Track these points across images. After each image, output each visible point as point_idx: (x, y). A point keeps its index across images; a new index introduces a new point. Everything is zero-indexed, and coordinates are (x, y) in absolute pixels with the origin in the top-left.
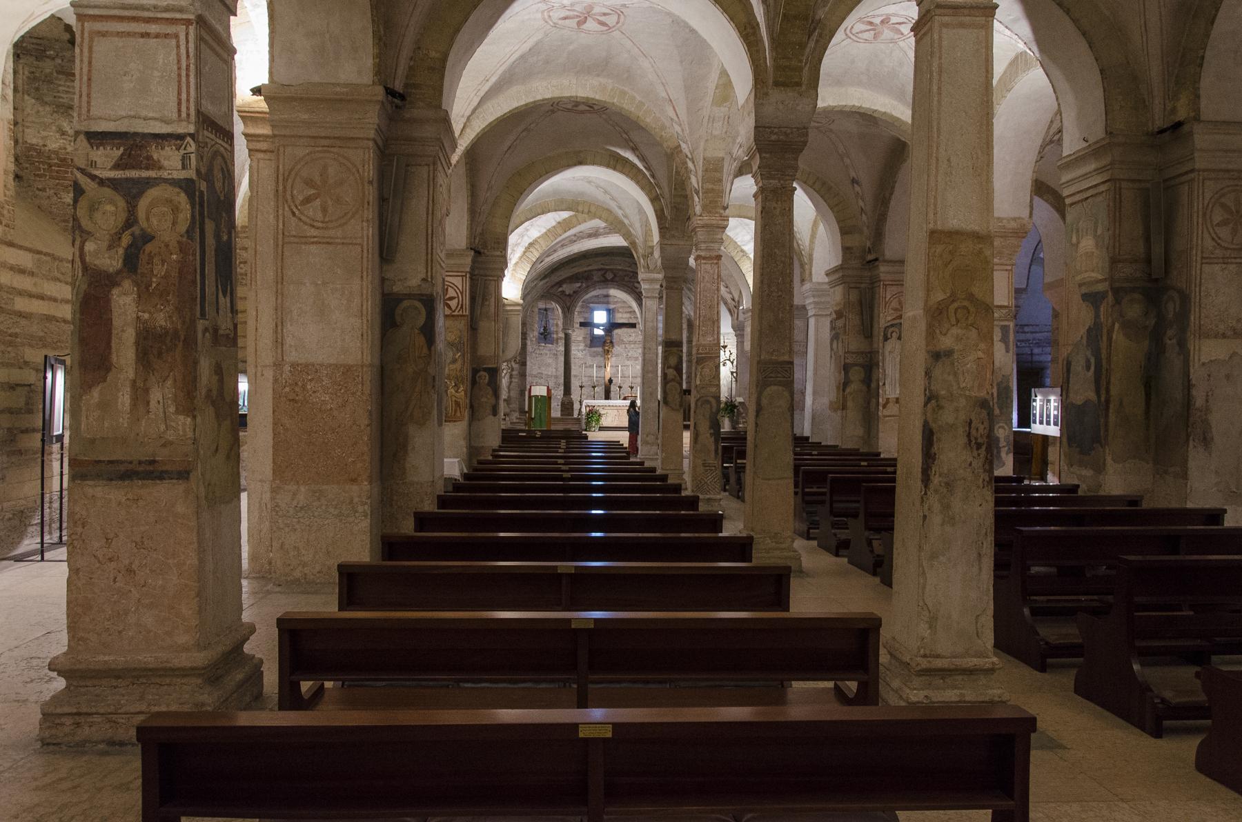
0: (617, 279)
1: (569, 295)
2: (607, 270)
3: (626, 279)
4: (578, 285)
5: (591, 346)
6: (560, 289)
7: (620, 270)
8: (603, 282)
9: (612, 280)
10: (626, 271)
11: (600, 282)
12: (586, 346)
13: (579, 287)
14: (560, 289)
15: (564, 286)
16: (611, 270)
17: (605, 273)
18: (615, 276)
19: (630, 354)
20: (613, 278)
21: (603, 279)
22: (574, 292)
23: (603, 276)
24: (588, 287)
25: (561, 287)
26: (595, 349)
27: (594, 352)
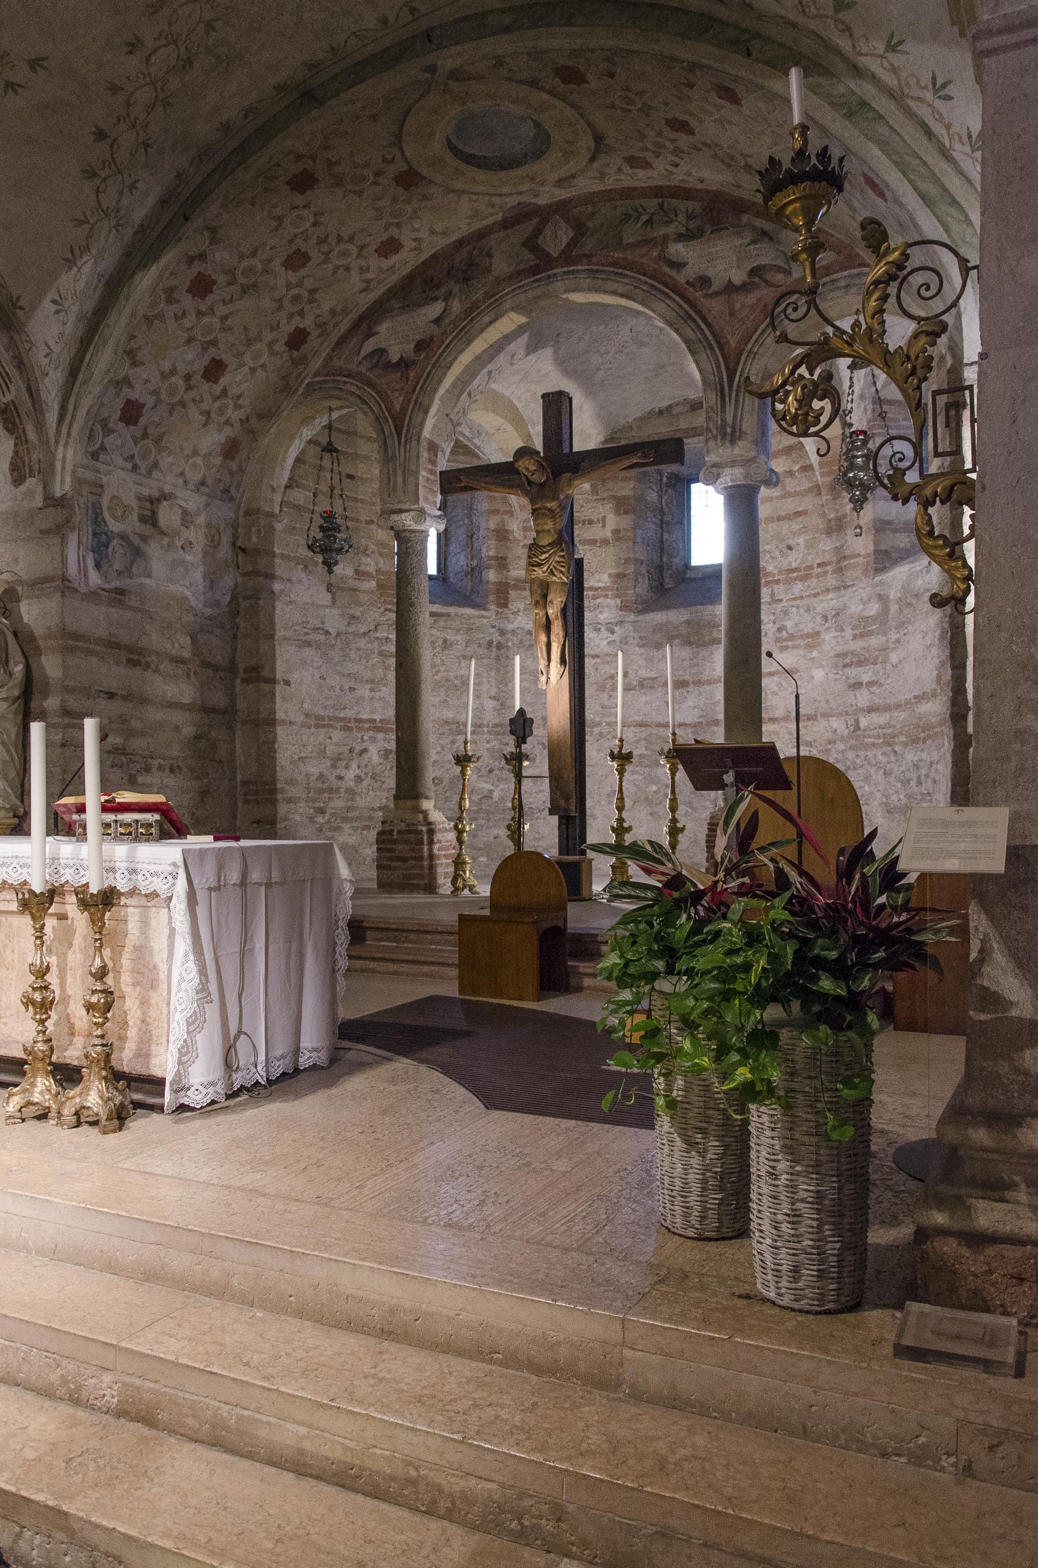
0: (589, 245)
1: (404, 365)
2: (543, 215)
3: (631, 234)
4: (435, 310)
5: (646, 607)
6: (370, 346)
7: (608, 196)
8: (534, 271)
9: (568, 257)
10: (628, 193)
11: (518, 274)
12: (624, 607)
13: (438, 321)
14: (370, 346)
15: (383, 328)
16: (561, 207)
17: (538, 231)
18: (580, 228)
19: (789, 624)
20: (573, 243)
21: (529, 258)
22: (421, 346)
23: (531, 244)
24: (471, 311)
25: (370, 334)
26: (659, 617)
27: (658, 628)
